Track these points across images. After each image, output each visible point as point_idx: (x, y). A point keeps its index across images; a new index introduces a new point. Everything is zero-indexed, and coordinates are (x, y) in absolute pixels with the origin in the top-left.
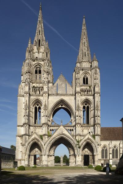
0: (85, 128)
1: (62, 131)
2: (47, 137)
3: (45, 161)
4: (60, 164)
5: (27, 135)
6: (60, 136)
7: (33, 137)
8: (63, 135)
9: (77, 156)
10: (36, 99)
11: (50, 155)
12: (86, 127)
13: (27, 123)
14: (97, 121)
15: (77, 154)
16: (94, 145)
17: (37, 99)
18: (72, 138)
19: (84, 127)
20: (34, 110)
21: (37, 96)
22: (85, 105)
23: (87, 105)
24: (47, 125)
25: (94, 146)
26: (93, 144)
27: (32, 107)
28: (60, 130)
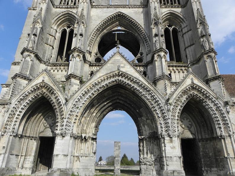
0: (175, 68)
1: (119, 67)
2: (78, 82)
3: (61, 157)
4: (112, 168)
5: (25, 78)
6: (113, 79)
7: (38, 81)
8: (120, 78)
9: (167, 138)
10: (65, 13)
11: (83, 135)
12: (176, 66)
13: (31, 49)
14: (207, 46)
15: (164, 133)
16: (212, 105)
17: (67, 12)
18: (147, 84)
19: (172, 66)
20: (58, 35)
21: (67, 8)
22: (167, 27)
23: (173, 27)
24: (81, 56)
25: (214, 108)
26: (209, 102)
27: (55, 28)
28: (111, 63)
